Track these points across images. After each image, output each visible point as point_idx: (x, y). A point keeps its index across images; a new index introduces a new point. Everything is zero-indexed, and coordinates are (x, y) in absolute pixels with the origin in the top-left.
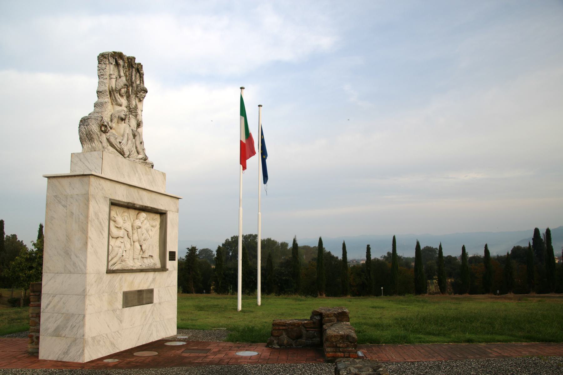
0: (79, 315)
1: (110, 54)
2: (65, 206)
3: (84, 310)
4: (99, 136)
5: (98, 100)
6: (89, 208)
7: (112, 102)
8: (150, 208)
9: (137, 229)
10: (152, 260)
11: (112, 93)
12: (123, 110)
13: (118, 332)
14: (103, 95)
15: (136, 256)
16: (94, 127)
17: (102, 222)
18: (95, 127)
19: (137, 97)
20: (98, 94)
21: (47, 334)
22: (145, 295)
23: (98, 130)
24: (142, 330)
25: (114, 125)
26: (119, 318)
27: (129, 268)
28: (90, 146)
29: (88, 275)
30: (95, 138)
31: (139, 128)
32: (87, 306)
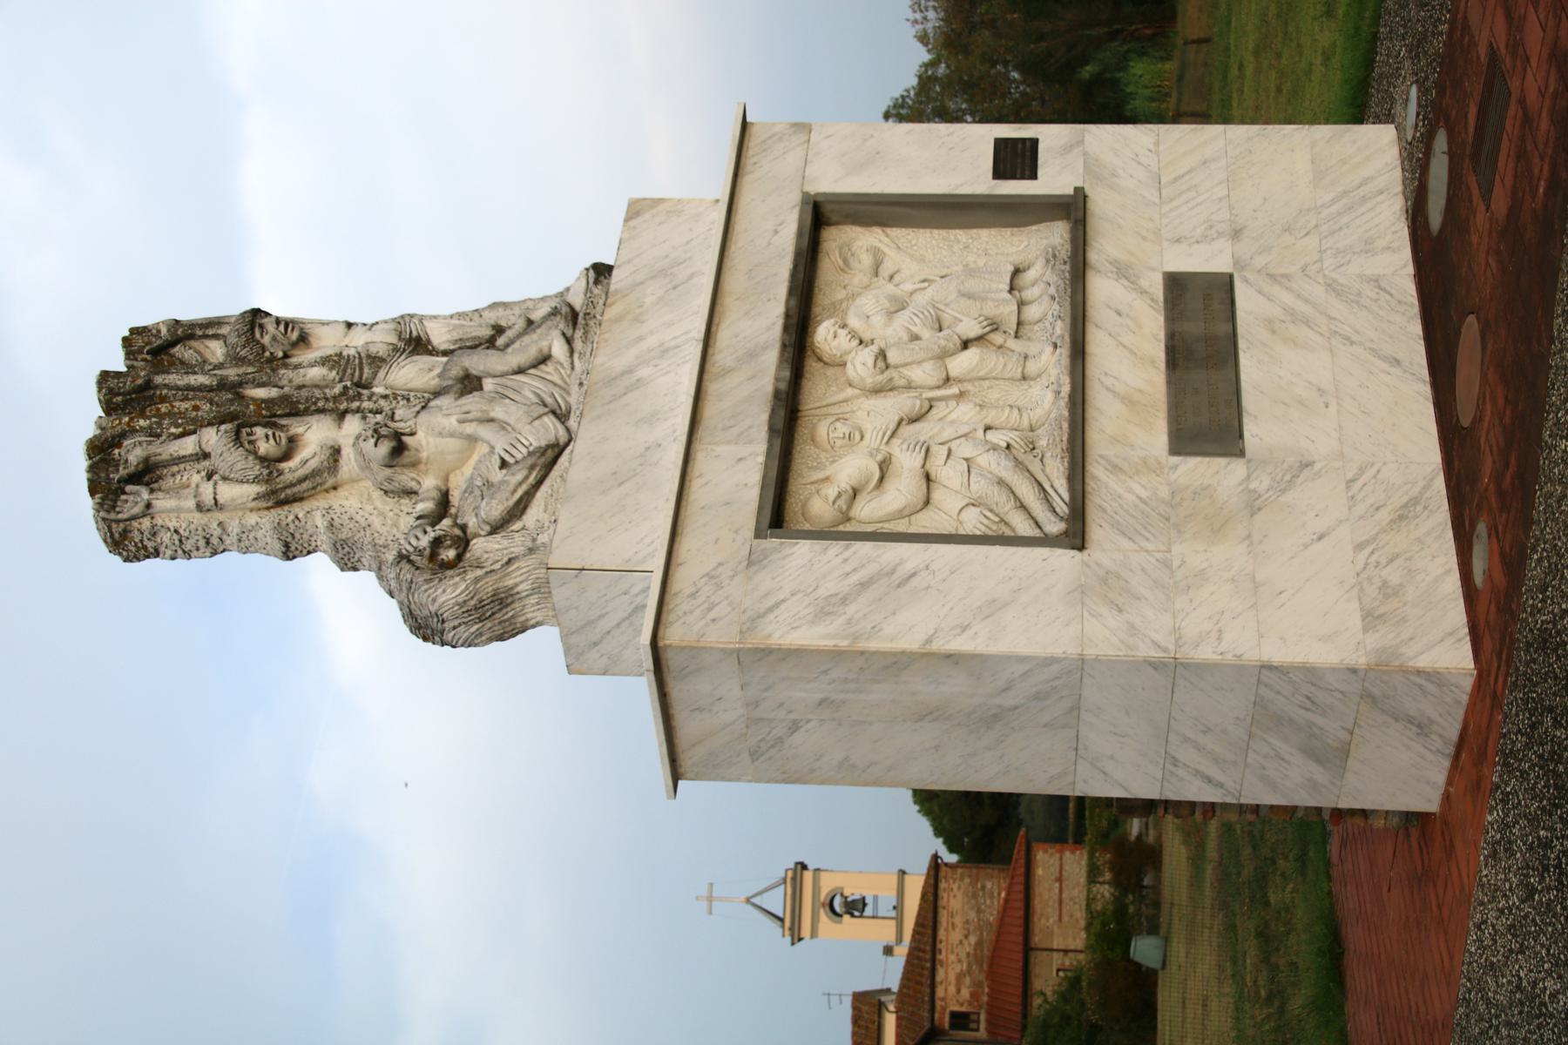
0: (1259, 681)
1: (102, 514)
2: (795, 727)
3: (1239, 669)
4: (484, 570)
5: (325, 552)
6: (796, 650)
7: (327, 491)
8: (793, 302)
9: (887, 367)
10: (1031, 274)
11: (283, 496)
12: (354, 445)
13: (1352, 481)
14: (297, 536)
15: (1009, 367)
16: (449, 594)
17: (855, 578)
18: (444, 591)
19: (286, 356)
20: (297, 553)
21: (1333, 783)
22: (1193, 328)
23: (457, 579)
24: (1352, 343)
25: (429, 483)
26: (1288, 477)
27: (1066, 413)
28: (533, 600)
29: (1090, 652)
30: (495, 587)
31: (429, 341)
32: (1221, 654)
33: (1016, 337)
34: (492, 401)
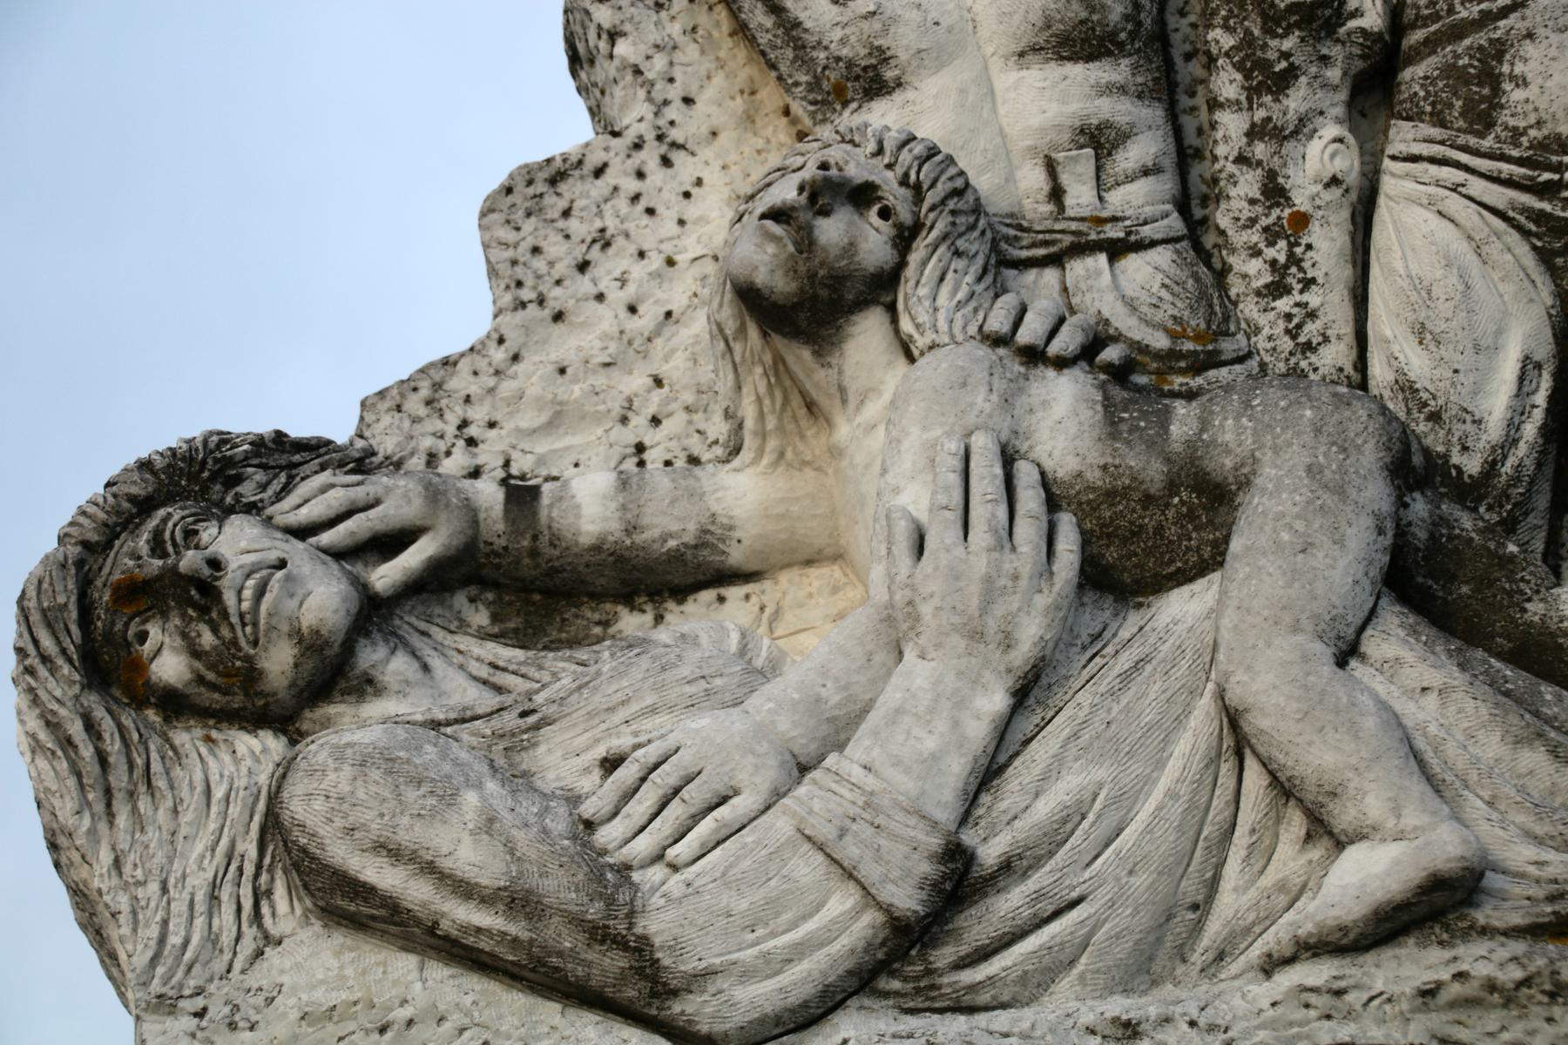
34: (976, 635)
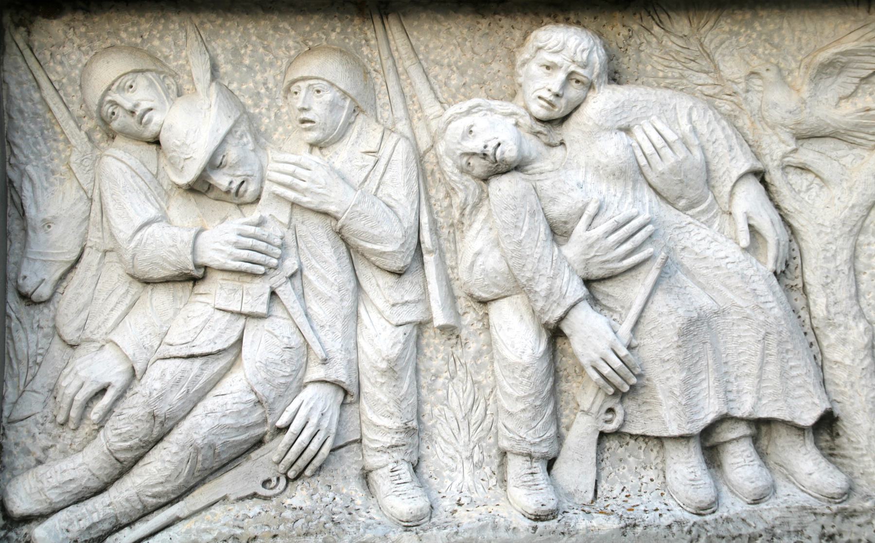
33: (603, 436)
